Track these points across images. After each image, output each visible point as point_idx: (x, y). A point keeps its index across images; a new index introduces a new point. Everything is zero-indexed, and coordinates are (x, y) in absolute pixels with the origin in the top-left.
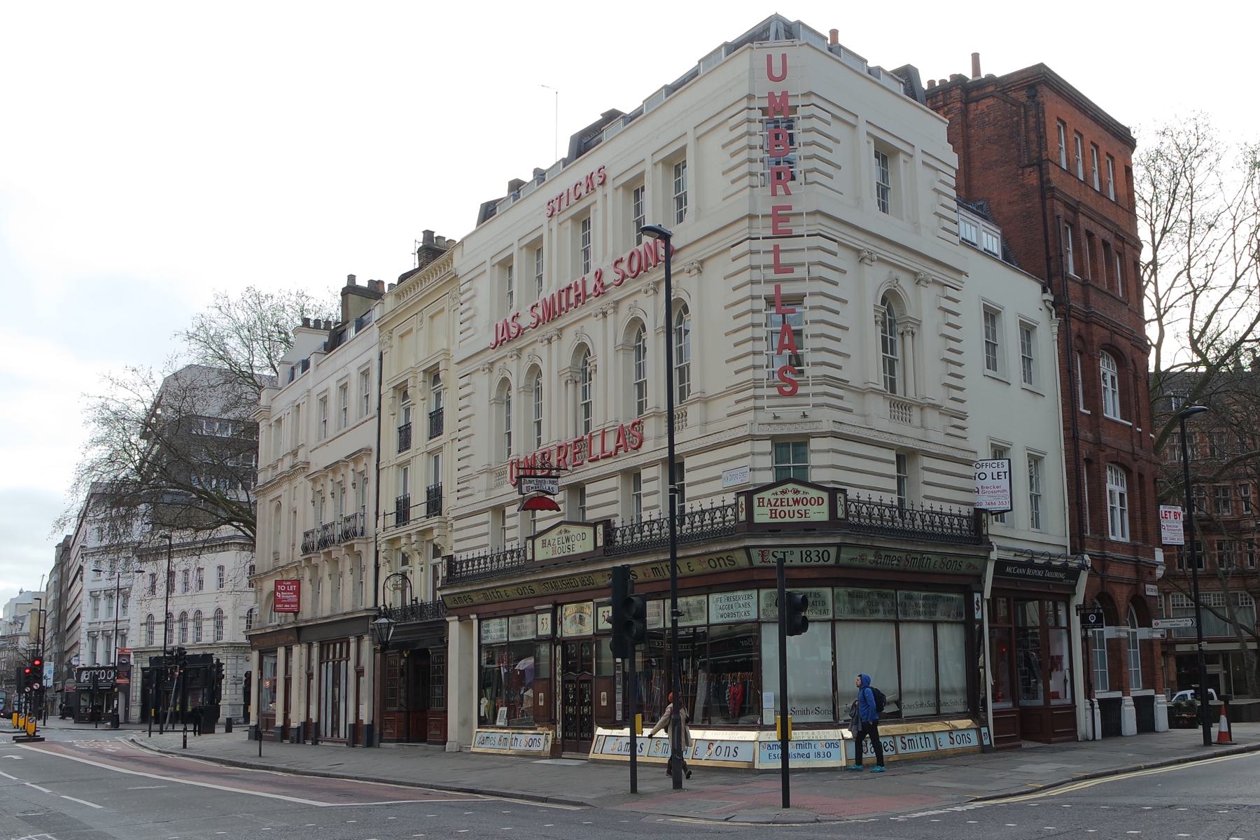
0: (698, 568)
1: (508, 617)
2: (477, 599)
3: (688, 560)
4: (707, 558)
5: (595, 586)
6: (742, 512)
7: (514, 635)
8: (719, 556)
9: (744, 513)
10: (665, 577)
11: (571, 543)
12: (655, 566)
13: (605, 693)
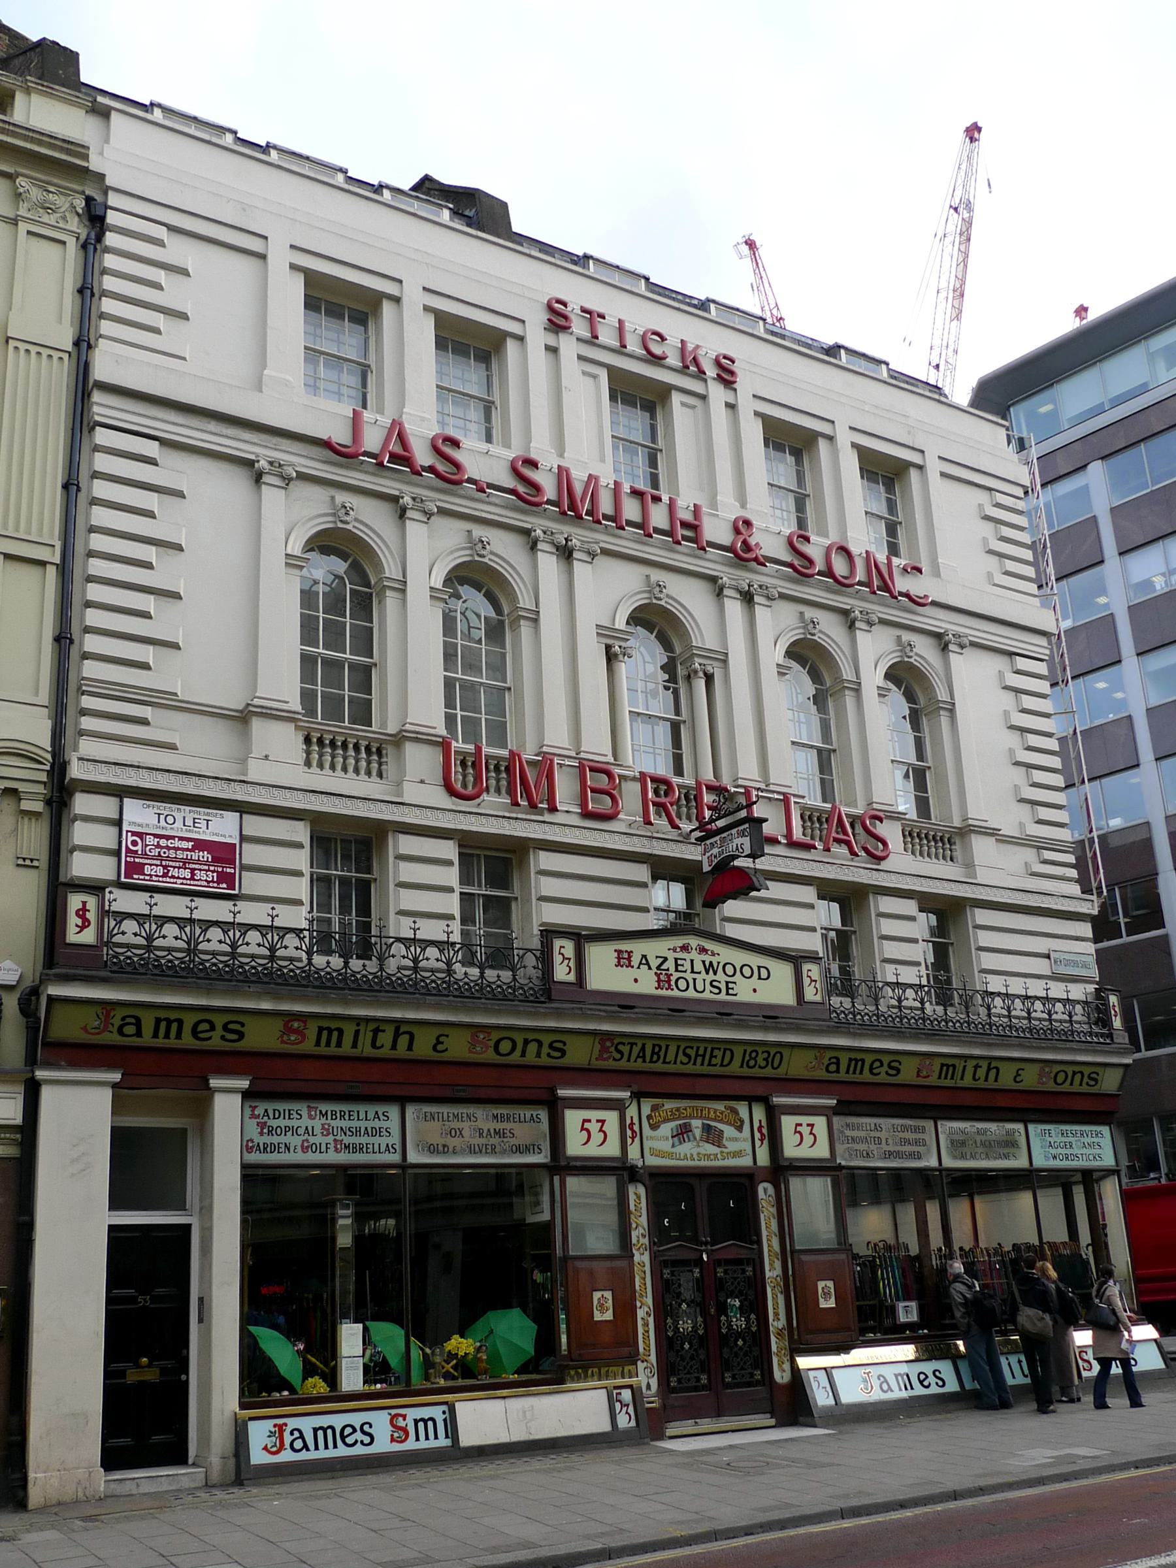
0: (1030, 1079)
1: (402, 1101)
2: (262, 1037)
3: (1022, 1065)
4: (1056, 1068)
5: (781, 1072)
6: (1116, 1016)
7: (432, 1149)
8: (1077, 1069)
9: (1118, 1018)
10: (960, 1084)
11: (720, 976)
12: (950, 1061)
13: (830, 1284)
